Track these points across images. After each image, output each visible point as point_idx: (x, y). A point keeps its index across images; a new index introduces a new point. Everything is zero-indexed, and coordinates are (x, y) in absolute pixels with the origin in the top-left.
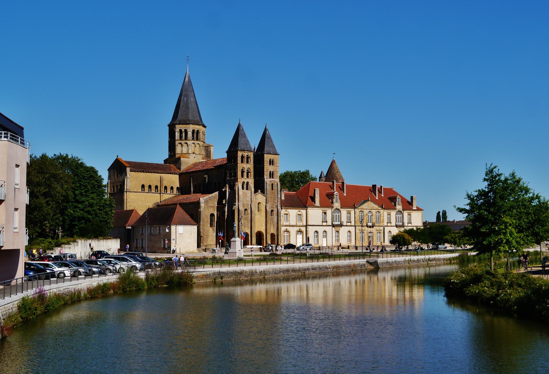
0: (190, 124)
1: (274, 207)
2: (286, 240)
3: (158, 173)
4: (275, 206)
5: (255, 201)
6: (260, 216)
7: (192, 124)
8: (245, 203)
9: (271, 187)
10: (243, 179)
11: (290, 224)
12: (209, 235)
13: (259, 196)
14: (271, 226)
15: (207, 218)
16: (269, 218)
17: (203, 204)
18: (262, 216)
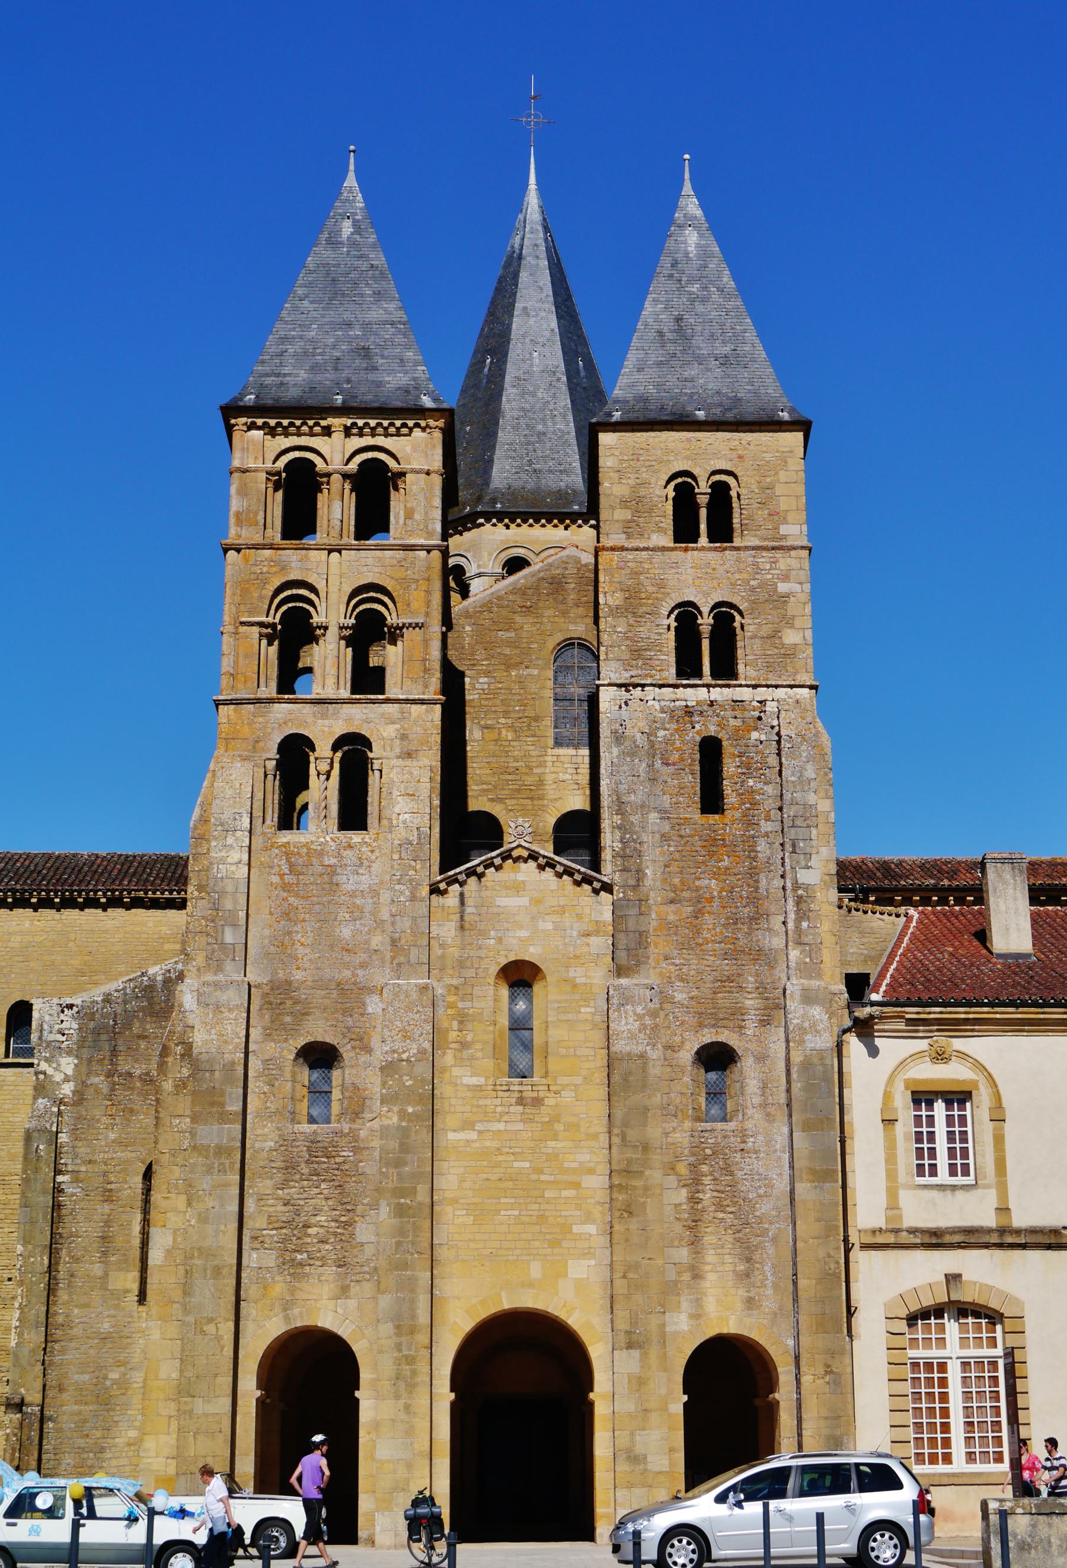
0: (482, 514)
1: (737, 1014)
2: (957, 1420)
3: (155, 904)
4: (751, 1003)
5: (454, 952)
6: (531, 1121)
7: (500, 516)
8: (298, 975)
9: (692, 781)
10: (281, 710)
11: (1003, 1210)
12: (123, 1384)
13: (518, 888)
14: (709, 1239)
15: (106, 1208)
16: (646, 1148)
17: (68, 1064)
18: (556, 1119)
